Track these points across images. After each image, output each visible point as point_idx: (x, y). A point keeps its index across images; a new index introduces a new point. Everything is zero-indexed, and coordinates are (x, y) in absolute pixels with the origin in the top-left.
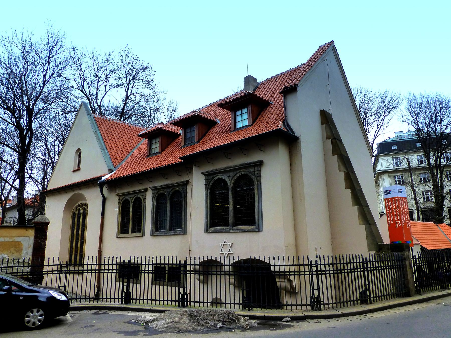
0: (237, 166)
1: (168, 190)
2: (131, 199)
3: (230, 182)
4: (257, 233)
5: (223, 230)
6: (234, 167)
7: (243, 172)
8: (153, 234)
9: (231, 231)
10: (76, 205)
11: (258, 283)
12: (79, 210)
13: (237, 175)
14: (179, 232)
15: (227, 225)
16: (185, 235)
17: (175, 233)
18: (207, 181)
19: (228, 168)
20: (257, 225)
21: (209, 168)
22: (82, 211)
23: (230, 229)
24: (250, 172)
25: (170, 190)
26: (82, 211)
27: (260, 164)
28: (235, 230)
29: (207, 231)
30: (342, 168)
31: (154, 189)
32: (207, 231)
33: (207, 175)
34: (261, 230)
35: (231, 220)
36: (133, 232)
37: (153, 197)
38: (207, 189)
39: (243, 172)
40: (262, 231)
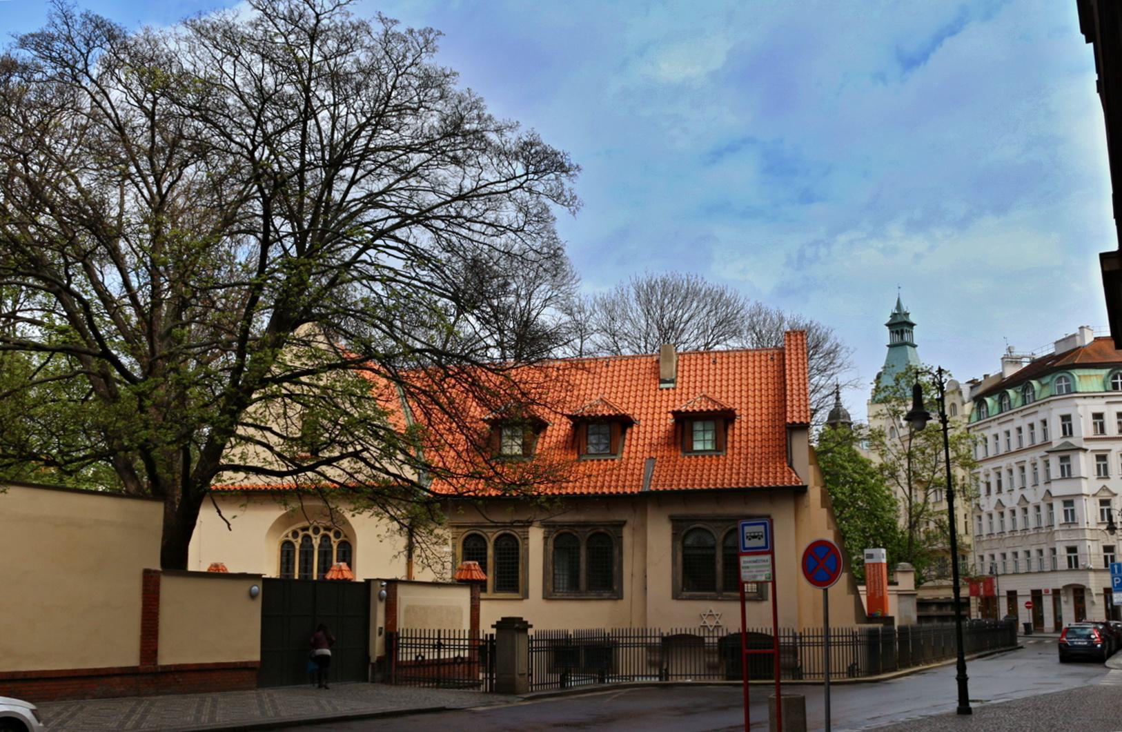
2: (491, 536)
3: (720, 536)
8: (548, 596)
10: (293, 528)
11: (754, 660)
12: (307, 538)
14: (606, 595)
15: (714, 589)
18: (674, 528)
21: (679, 511)
22: (316, 542)
26: (316, 542)
29: (676, 596)
30: (832, 525)
31: (545, 525)
32: (676, 596)
33: (674, 520)
35: (719, 583)
36: (494, 591)
37: (546, 539)
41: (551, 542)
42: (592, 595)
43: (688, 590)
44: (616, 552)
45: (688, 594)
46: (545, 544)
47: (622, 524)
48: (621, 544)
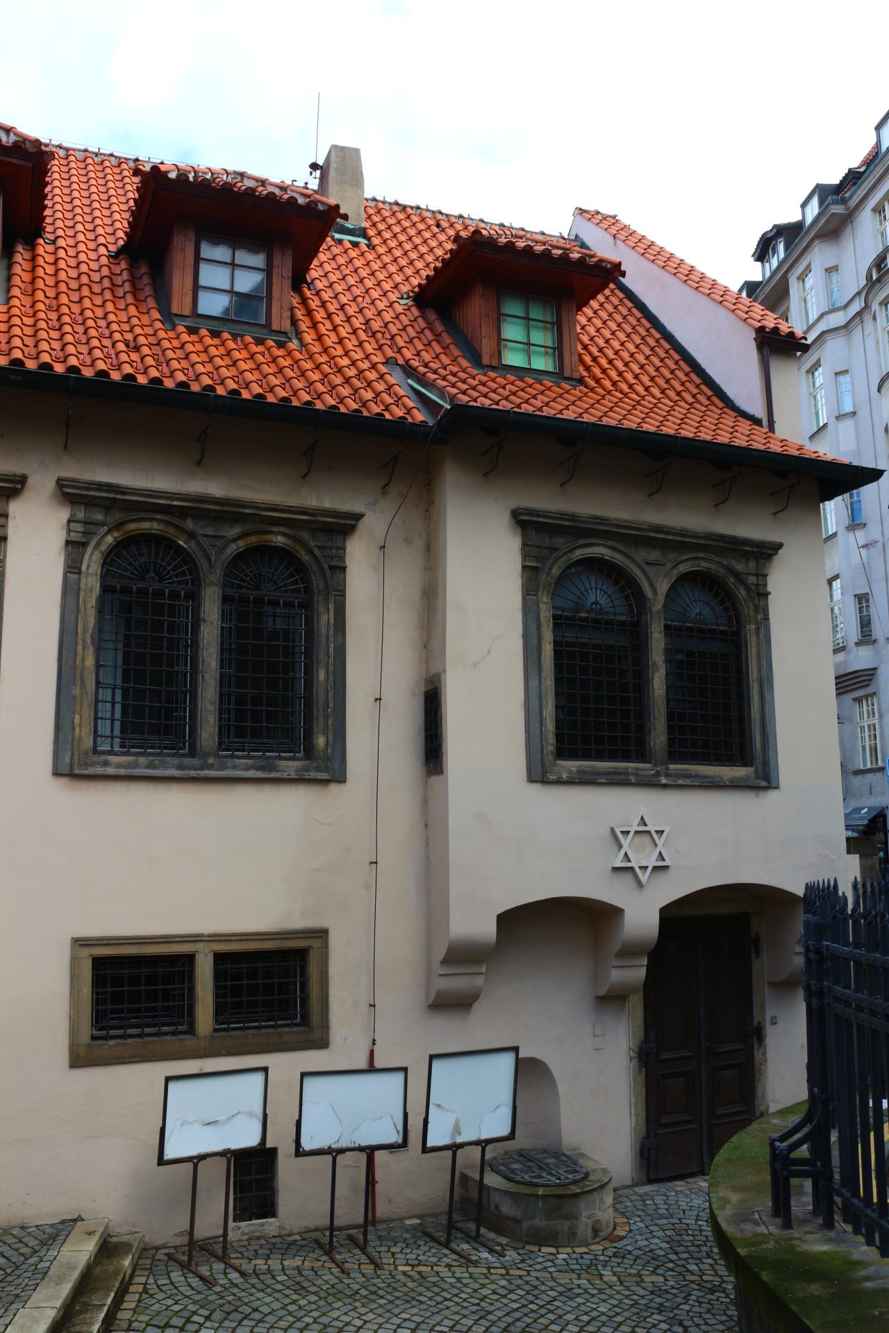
0: (696, 536)
1: (210, 531)
3: (658, 588)
4: (761, 793)
5: (626, 774)
6: (684, 533)
7: (704, 564)
9: (664, 781)
13: (683, 568)
14: (290, 766)
15: (642, 756)
16: (334, 788)
17: (262, 768)
19: (658, 529)
20: (759, 762)
21: (546, 500)
23: (658, 774)
24: (738, 576)
25: (236, 530)
27: (766, 552)
28: (677, 776)
29: (539, 774)
31: (69, 493)
32: (539, 774)
34: (774, 785)
35: (658, 736)
38: (529, 590)
39: (704, 564)
40: (777, 787)
41: (92, 562)
42: (241, 765)
43: (573, 756)
44: (325, 619)
45: (572, 766)
46: (73, 567)
47: (344, 526)
48: (342, 593)
